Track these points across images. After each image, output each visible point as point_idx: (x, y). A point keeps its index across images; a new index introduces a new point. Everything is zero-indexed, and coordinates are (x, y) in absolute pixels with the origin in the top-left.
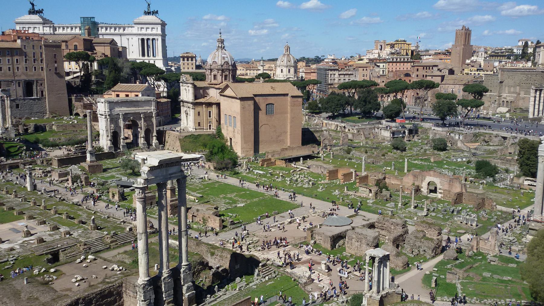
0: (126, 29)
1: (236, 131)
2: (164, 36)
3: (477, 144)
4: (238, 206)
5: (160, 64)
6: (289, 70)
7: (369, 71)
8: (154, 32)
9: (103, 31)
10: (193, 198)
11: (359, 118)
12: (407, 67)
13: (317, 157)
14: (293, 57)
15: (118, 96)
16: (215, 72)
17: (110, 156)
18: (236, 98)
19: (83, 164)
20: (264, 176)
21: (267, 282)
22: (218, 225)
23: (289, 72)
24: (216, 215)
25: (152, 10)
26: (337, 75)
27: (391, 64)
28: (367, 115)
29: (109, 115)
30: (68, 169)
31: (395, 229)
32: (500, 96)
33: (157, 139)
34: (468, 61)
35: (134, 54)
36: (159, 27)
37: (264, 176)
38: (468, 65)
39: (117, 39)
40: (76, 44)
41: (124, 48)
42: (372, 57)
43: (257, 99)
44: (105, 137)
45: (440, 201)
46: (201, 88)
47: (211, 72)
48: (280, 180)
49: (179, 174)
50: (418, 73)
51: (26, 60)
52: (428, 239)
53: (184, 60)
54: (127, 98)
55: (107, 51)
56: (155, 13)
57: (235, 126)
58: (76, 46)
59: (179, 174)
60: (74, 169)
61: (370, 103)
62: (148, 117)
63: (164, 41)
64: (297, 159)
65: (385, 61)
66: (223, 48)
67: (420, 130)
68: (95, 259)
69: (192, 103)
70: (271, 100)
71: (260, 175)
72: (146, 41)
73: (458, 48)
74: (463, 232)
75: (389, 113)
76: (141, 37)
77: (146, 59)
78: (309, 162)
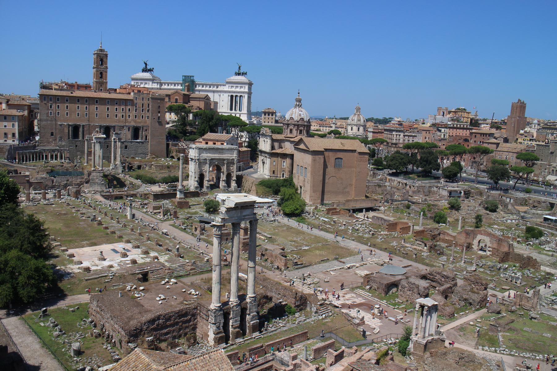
1: (306, 180)
2: (250, 94)
3: (527, 208)
5: (244, 118)
6: (359, 128)
8: (242, 90)
9: (200, 88)
10: (263, 238)
12: (466, 133)
13: (379, 210)
17: (195, 194)
19: (173, 199)
21: (323, 319)
23: (358, 130)
24: (282, 256)
25: (241, 71)
27: (451, 130)
28: (426, 174)
30: (161, 203)
34: (522, 132)
35: (224, 109)
36: (247, 87)
38: (522, 135)
39: (210, 95)
40: (177, 97)
41: (216, 103)
44: (193, 178)
48: (343, 228)
49: (252, 216)
51: (136, 109)
53: (265, 115)
55: (202, 105)
56: (244, 74)
57: (306, 176)
58: (177, 99)
59: (252, 216)
60: (166, 203)
62: (230, 163)
63: (249, 98)
64: (360, 210)
65: (446, 126)
66: (300, 106)
68: (176, 283)
70: (340, 155)
71: (325, 222)
72: (234, 98)
73: (513, 119)
74: (508, 288)
75: (448, 174)
76: (230, 94)
77: (233, 113)
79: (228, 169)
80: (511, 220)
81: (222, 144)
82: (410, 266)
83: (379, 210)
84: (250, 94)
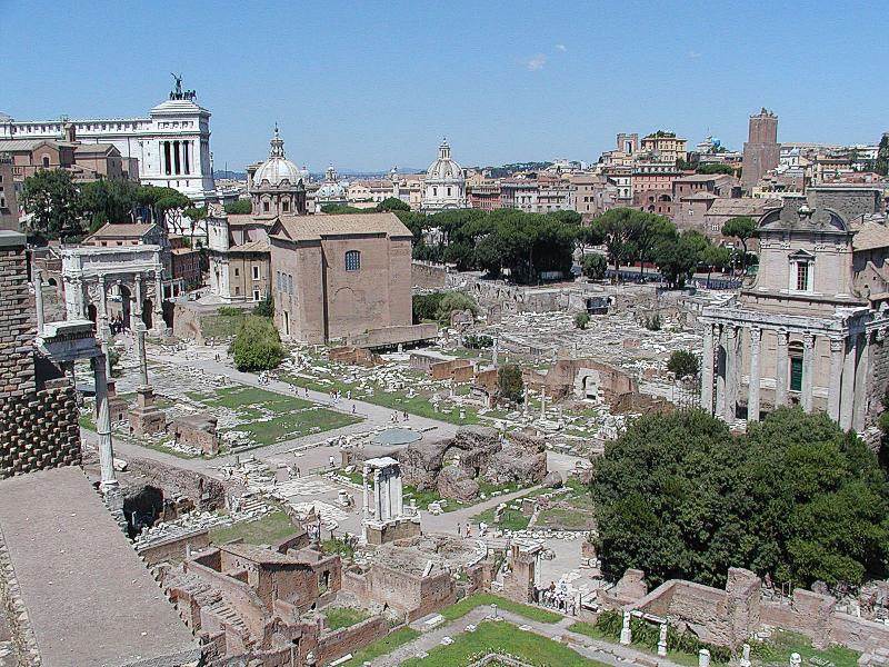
0: (139, 125)
2: (204, 137)
8: (187, 129)
16: (266, 199)
23: (449, 194)
24: (209, 432)
27: (639, 179)
35: (152, 170)
36: (196, 121)
39: (121, 145)
40: (48, 156)
41: (134, 162)
54: (105, 248)
62: (146, 278)
63: (204, 144)
70: (354, 245)
72: (172, 147)
79: (143, 293)
84: (204, 137)
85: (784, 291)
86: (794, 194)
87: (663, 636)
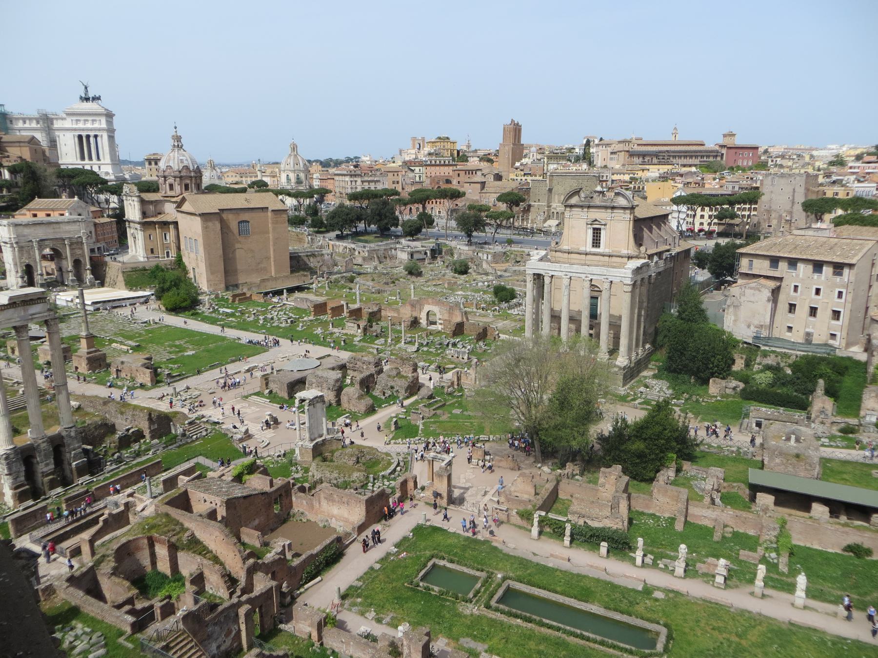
4: (186, 354)
7: (400, 176)
8: (96, 125)
9: (20, 124)
11: (376, 237)
12: (447, 171)
13: (308, 288)
14: (303, 159)
15: (35, 215)
16: (171, 180)
18: (195, 215)
20: (232, 315)
22: (149, 379)
25: (91, 95)
26: (359, 182)
28: (384, 232)
29: (17, 243)
31: (367, 369)
32: (549, 206)
33: (93, 273)
34: (517, 164)
35: (69, 156)
36: (103, 120)
37: (232, 315)
42: (407, 159)
43: (225, 216)
44: (13, 273)
45: (439, 332)
46: (151, 202)
47: (165, 180)
48: (251, 319)
50: (459, 179)
52: (403, 377)
53: (150, 164)
56: (96, 99)
61: (386, 217)
62: (76, 244)
63: (111, 138)
64: (279, 293)
65: (421, 164)
66: (180, 147)
67: (444, 249)
69: (139, 223)
70: (245, 216)
71: (228, 315)
73: (507, 148)
74: (453, 366)
75: (408, 230)
76: (77, 133)
77: (87, 165)
78: (297, 294)
80: (484, 282)
81: (62, 215)
82: (329, 355)
83: (308, 288)
84: (111, 132)
85: (582, 249)
86: (538, 178)
87: (568, 532)
